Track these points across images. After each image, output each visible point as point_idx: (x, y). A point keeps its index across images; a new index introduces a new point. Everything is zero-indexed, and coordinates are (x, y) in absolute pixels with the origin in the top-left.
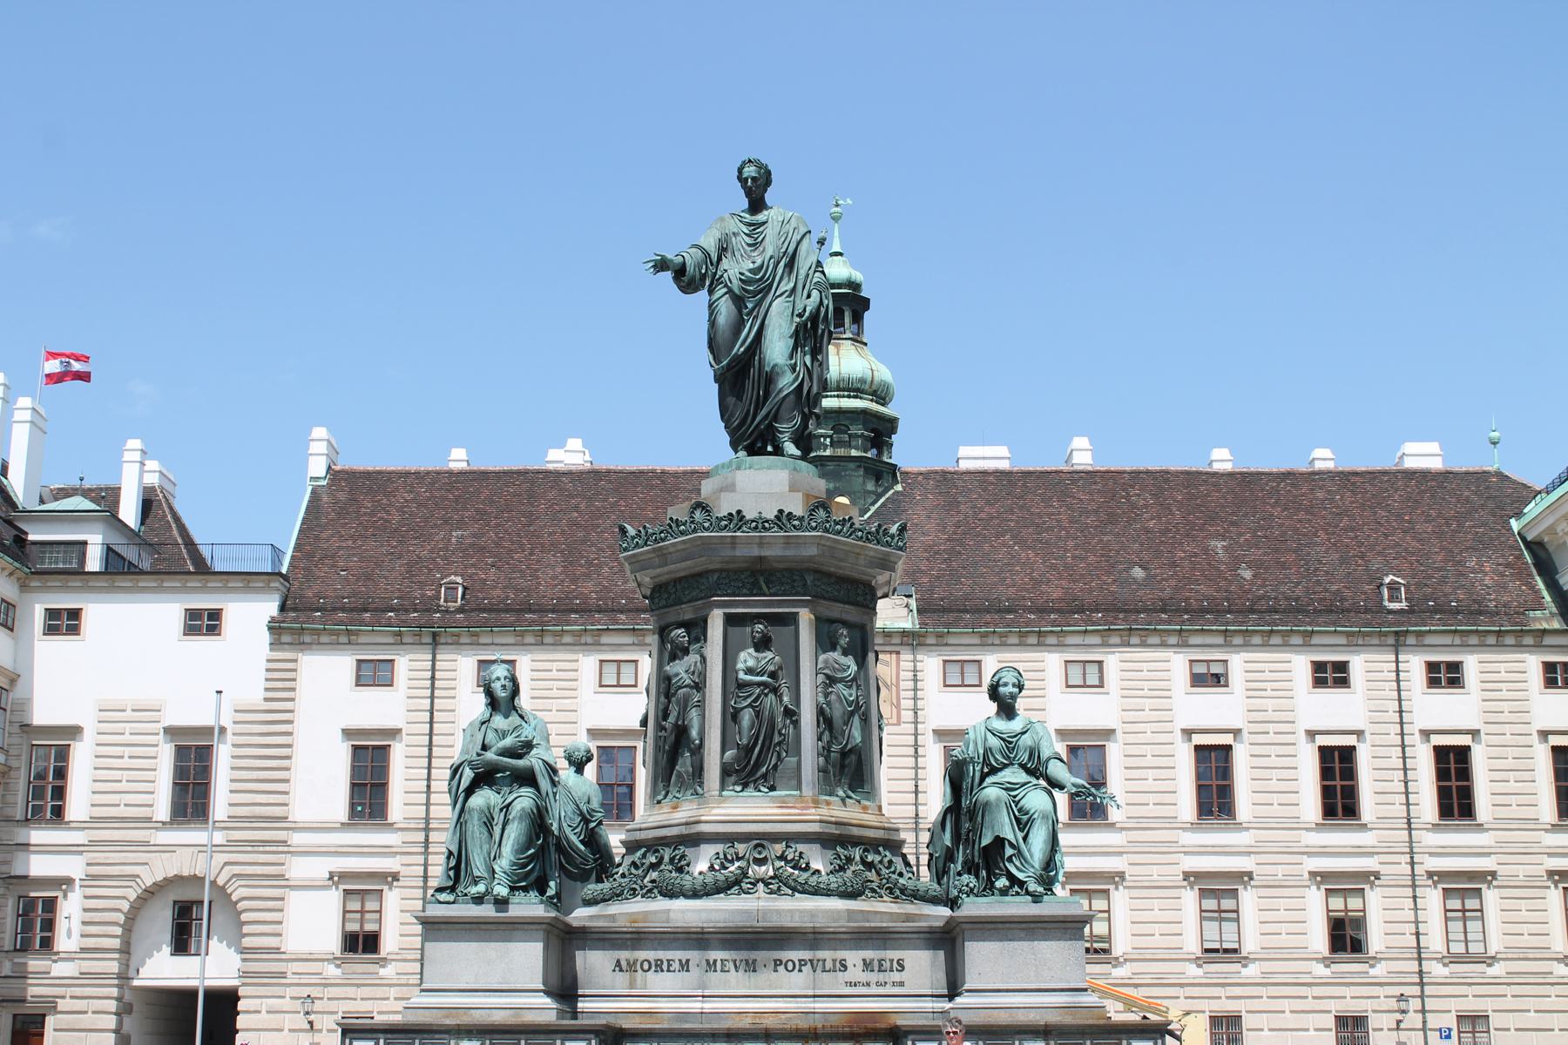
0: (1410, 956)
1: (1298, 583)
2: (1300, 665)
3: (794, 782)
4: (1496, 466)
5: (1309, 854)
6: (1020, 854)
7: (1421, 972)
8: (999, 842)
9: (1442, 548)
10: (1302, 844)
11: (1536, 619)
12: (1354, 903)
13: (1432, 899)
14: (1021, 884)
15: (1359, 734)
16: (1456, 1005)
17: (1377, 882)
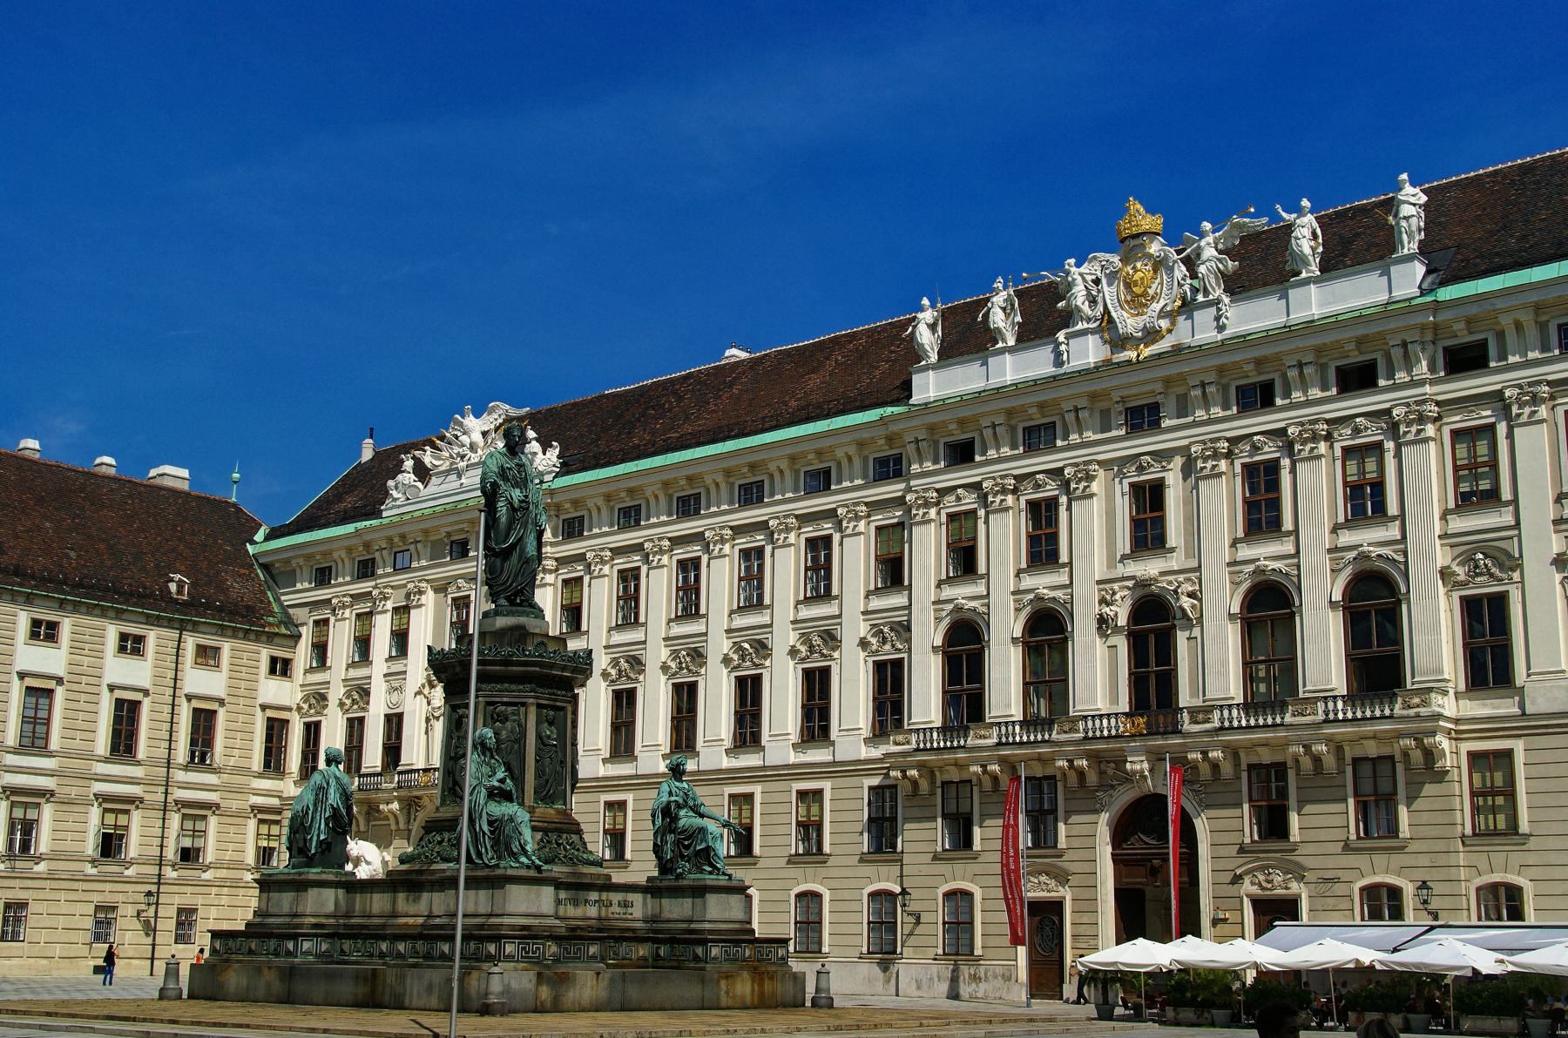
0: (153, 862)
1: (111, 568)
2: (112, 631)
3: (561, 802)
4: (234, 499)
5: (96, 780)
6: (715, 855)
7: (160, 875)
8: (708, 849)
9: (205, 557)
10: (93, 772)
11: (270, 625)
12: (122, 820)
13: (175, 820)
14: (718, 869)
15: (146, 693)
16: (178, 901)
17: (140, 806)
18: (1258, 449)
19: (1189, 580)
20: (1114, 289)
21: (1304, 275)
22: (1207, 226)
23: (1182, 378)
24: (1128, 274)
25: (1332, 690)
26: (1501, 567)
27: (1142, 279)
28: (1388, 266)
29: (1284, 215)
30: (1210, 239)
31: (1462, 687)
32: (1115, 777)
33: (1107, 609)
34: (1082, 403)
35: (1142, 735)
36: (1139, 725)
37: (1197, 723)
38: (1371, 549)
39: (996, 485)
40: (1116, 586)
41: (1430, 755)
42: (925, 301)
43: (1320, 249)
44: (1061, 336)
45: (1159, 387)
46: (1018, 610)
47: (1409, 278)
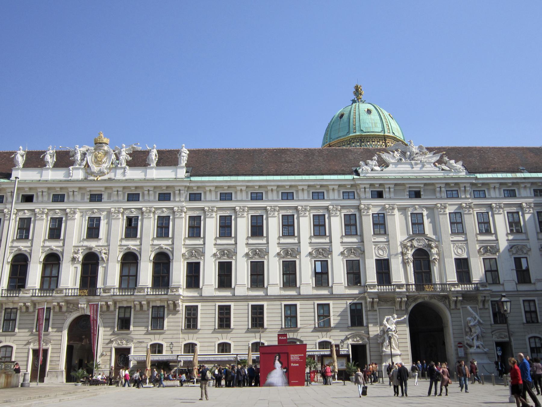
18: (132, 213)
19: (105, 249)
20: (90, 157)
21: (152, 166)
22: (124, 145)
23: (111, 188)
24: (96, 154)
25: (147, 286)
26: (199, 255)
27: (101, 156)
28: (177, 168)
29: (148, 148)
30: (124, 149)
31: (185, 287)
32: (72, 309)
33: (76, 255)
34: (76, 190)
35: (86, 295)
36: (85, 292)
37: (106, 293)
38: (164, 246)
39: (40, 211)
40: (80, 249)
41: (175, 305)
42: (21, 147)
43: (157, 159)
44: (71, 168)
45: (103, 189)
46: (42, 253)
47: (182, 173)
